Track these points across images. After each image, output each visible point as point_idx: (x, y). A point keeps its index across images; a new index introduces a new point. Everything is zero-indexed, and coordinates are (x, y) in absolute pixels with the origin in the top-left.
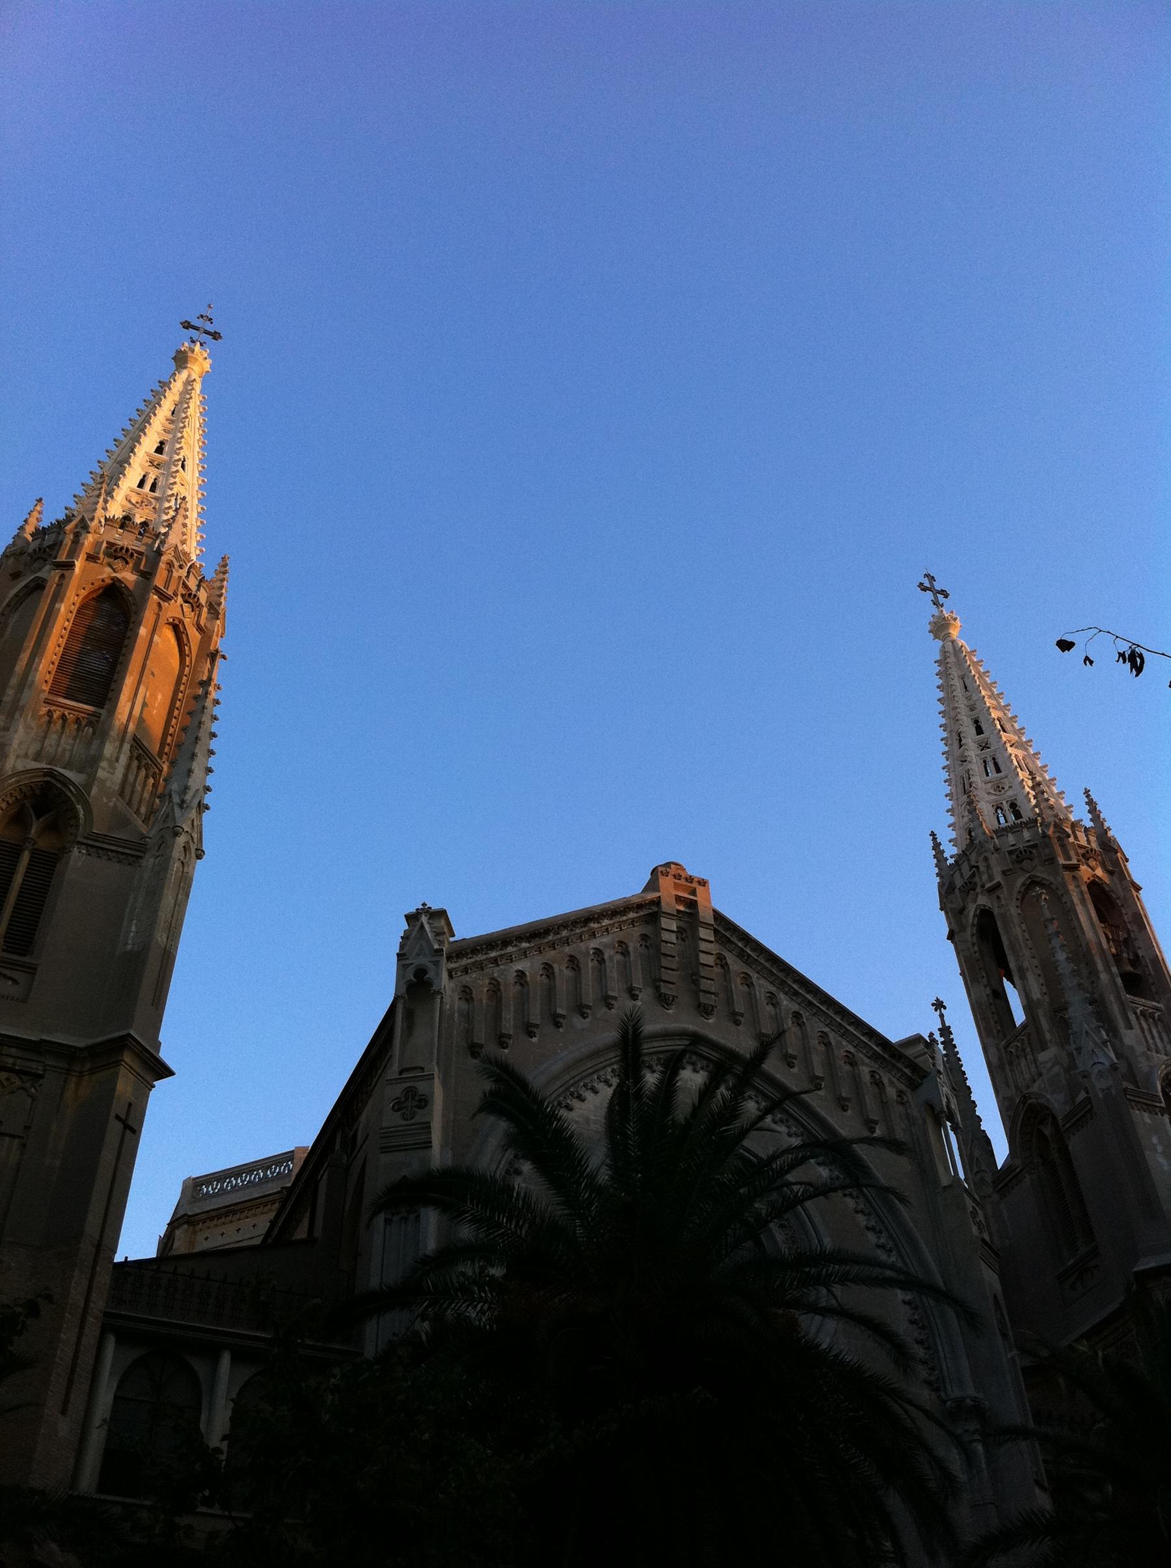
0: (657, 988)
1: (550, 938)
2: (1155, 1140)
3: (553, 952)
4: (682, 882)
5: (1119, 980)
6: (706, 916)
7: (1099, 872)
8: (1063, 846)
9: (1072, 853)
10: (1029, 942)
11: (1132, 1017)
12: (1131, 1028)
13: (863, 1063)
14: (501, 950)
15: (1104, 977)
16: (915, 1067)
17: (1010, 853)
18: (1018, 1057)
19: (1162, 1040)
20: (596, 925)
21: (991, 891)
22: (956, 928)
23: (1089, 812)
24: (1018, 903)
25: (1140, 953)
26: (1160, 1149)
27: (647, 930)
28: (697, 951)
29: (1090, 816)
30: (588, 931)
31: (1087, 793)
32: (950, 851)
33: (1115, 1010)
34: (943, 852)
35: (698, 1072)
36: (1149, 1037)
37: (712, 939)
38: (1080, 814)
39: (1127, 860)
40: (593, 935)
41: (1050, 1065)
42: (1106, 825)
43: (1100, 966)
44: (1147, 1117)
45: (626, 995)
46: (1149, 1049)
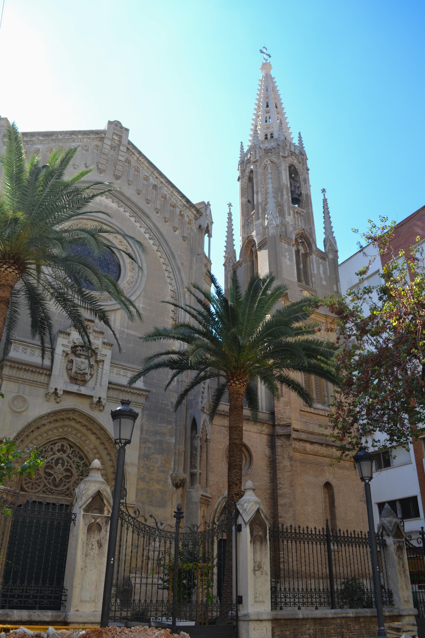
0: (98, 166)
1: (53, 138)
2: (287, 254)
3: (54, 144)
4: (118, 128)
5: (290, 199)
6: (124, 142)
7: (296, 161)
8: (284, 149)
9: (286, 152)
10: (263, 182)
11: (291, 212)
12: (289, 215)
13: (179, 208)
14: (30, 138)
15: (285, 197)
16: (198, 211)
17: (265, 150)
18: (250, 223)
19: (301, 223)
20: (75, 137)
21: (254, 162)
22: (241, 177)
23: (299, 140)
24: (263, 168)
25: (302, 192)
26: (288, 257)
27: (99, 144)
28: (118, 154)
29: (298, 142)
30: (72, 138)
31: (299, 134)
32: (246, 149)
33: (286, 209)
34: (243, 149)
35: (107, 199)
36: (296, 220)
37: (125, 151)
38: (296, 141)
39: (307, 159)
40: (74, 141)
41: (258, 225)
42: (304, 146)
43: (285, 193)
44: (286, 246)
45: (84, 166)
46: (295, 224)
